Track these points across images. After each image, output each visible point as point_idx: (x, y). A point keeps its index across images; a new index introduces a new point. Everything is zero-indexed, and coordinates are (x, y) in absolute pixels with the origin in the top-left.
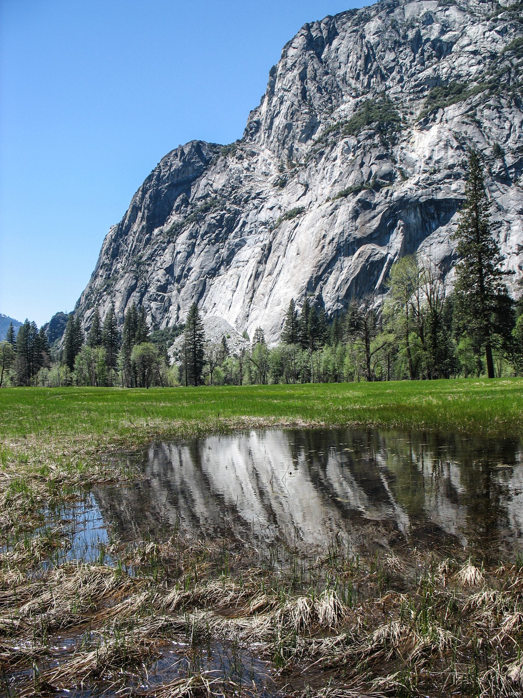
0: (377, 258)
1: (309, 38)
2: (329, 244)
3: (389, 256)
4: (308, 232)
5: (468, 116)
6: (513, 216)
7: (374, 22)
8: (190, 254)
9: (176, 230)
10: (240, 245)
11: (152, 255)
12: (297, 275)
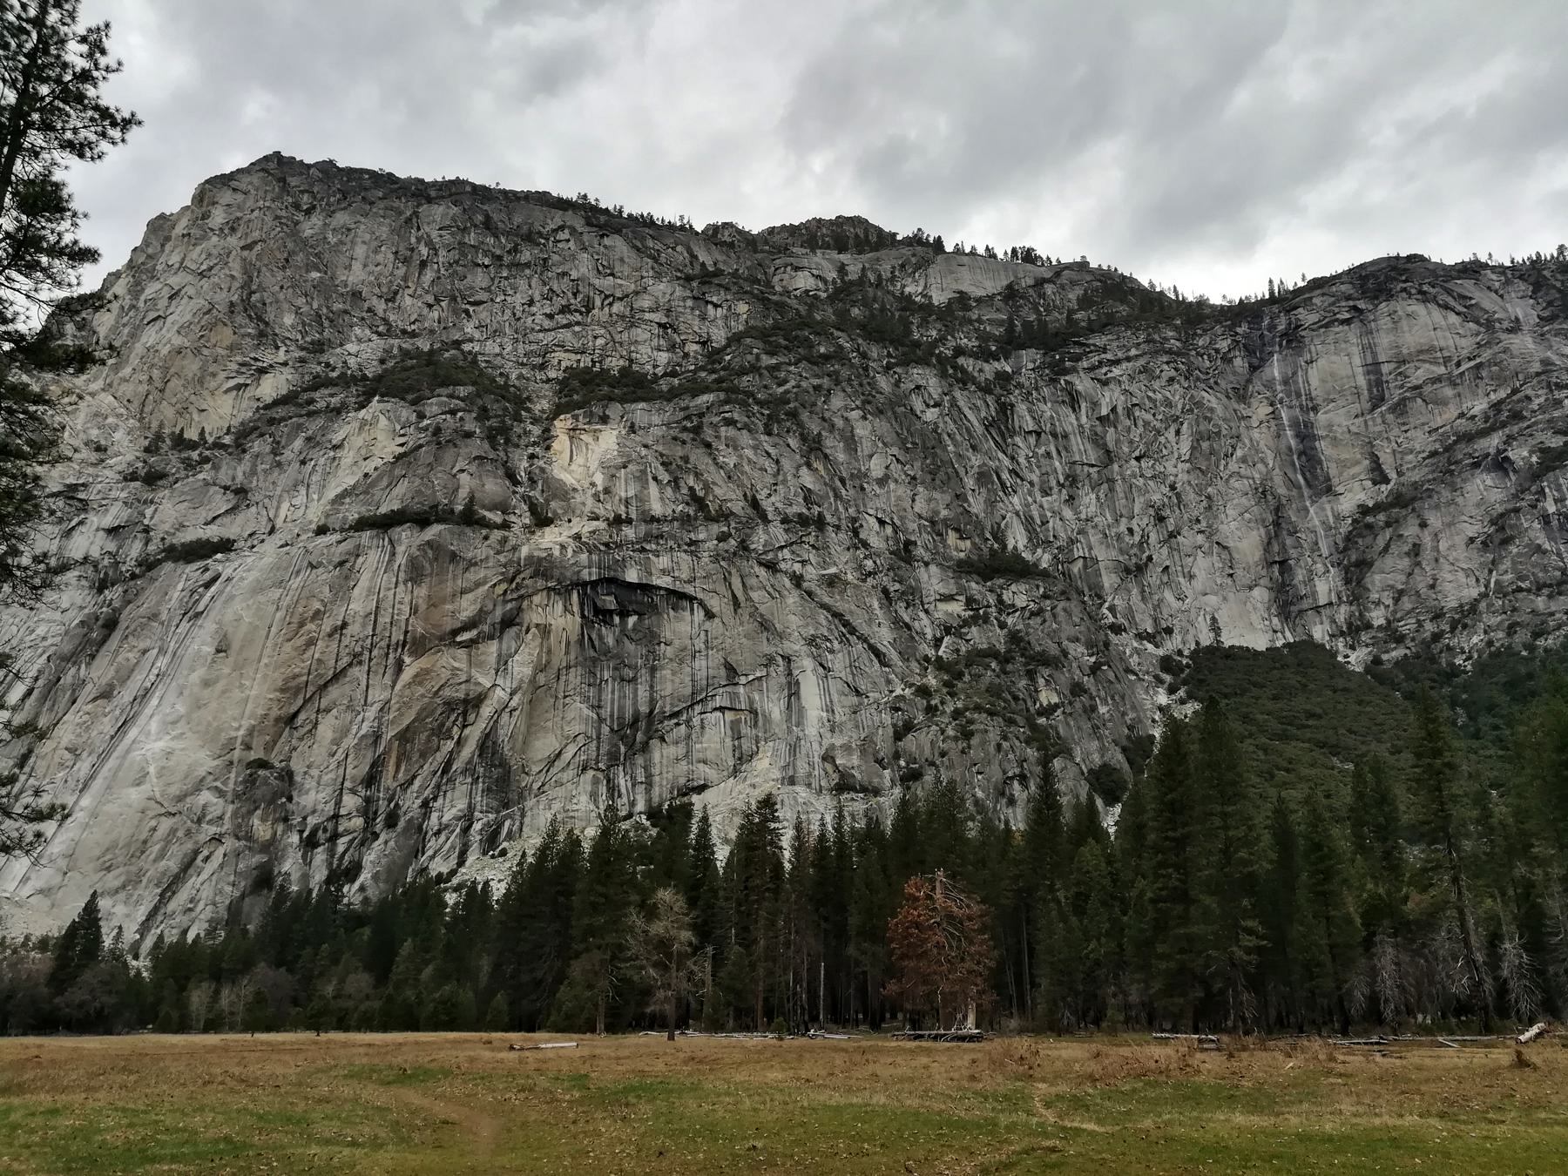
2: (330, 635)
4: (260, 598)
5: (685, 429)
6: (797, 647)
7: (441, 208)
12: (213, 705)
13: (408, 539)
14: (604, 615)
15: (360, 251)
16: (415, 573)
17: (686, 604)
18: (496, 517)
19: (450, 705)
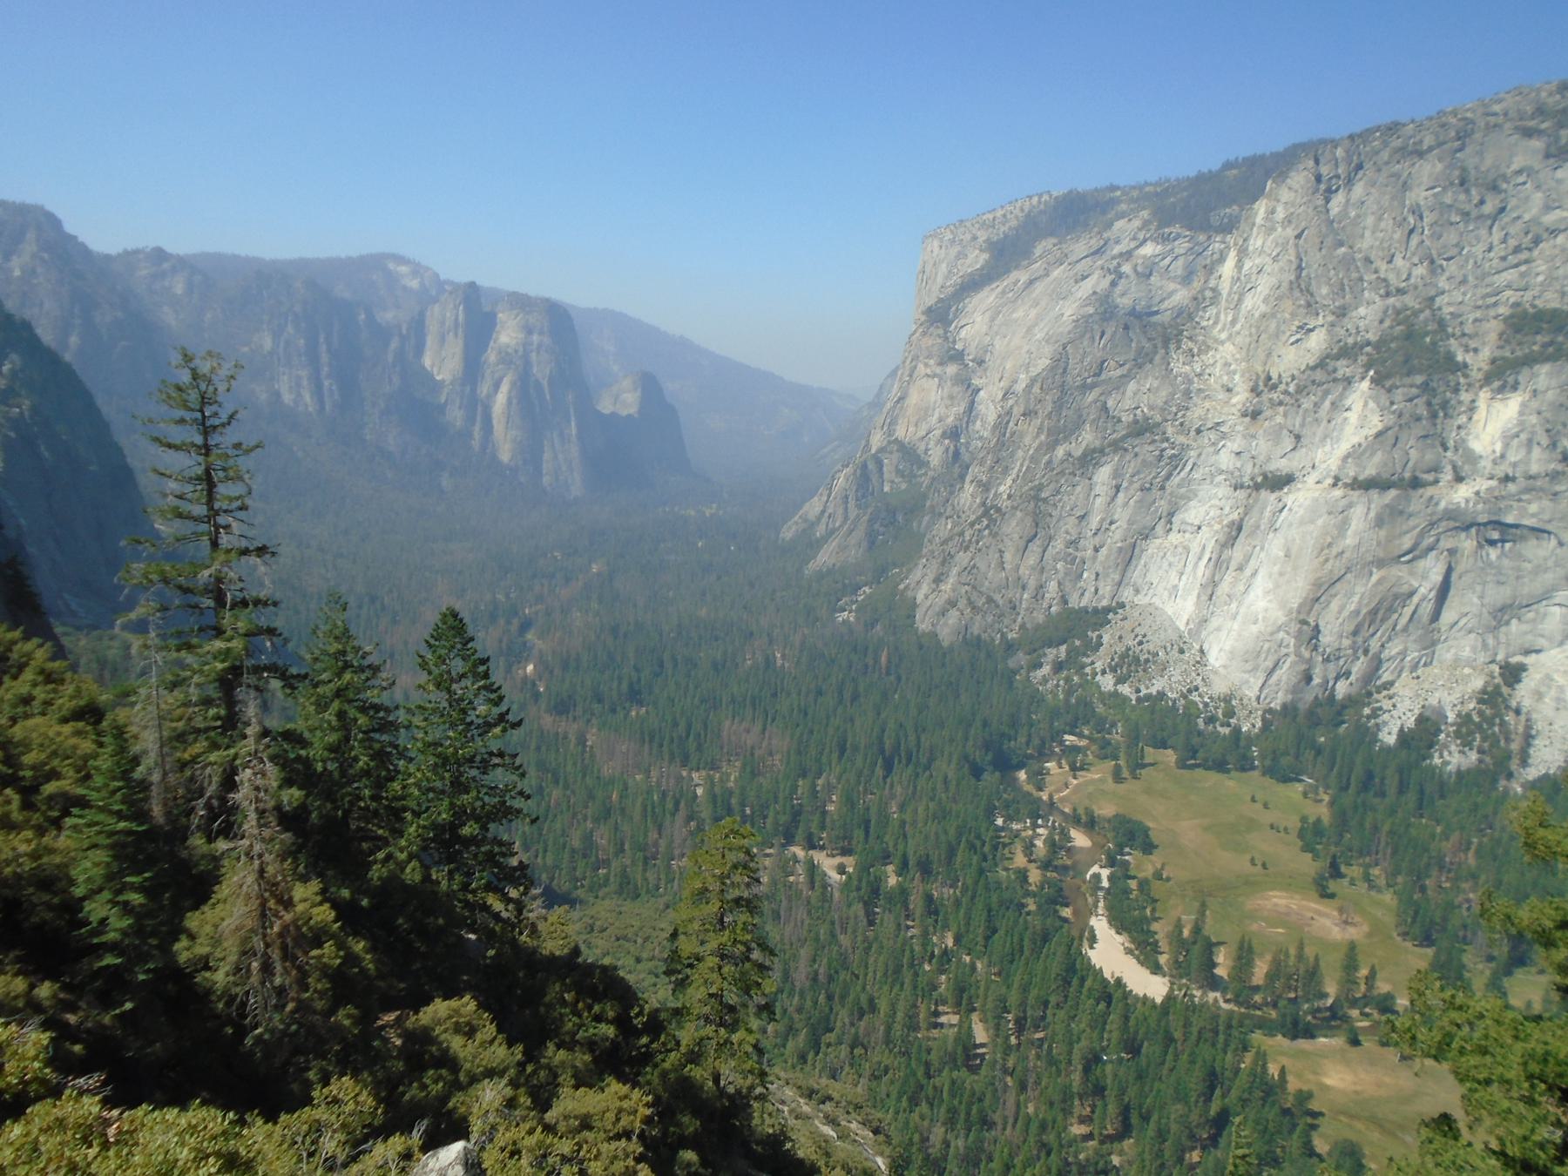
3: (1422, 590)
13: (1379, 500)
14: (1492, 543)
15: (1370, 220)
16: (1379, 522)
17: (1546, 535)
18: (1430, 477)
19: (1396, 597)
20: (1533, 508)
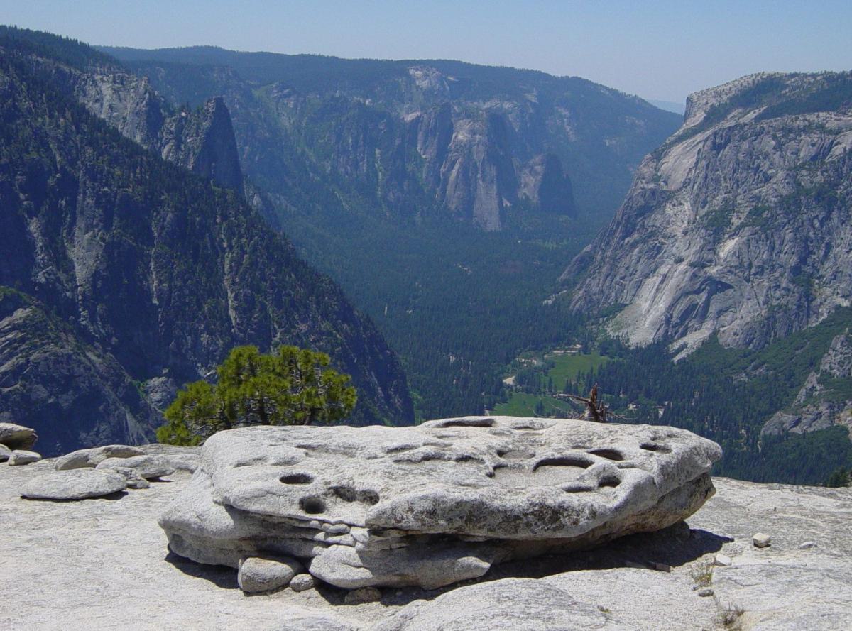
0: (695, 303)
1: (714, 143)
8: (638, 262)
9: (634, 245)
10: (662, 263)
11: (621, 257)
18: (709, 264)
20: (730, 278)
